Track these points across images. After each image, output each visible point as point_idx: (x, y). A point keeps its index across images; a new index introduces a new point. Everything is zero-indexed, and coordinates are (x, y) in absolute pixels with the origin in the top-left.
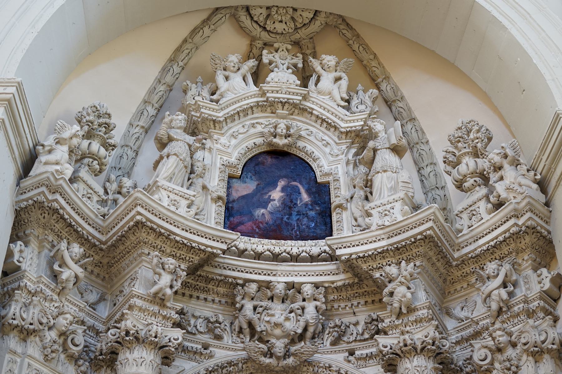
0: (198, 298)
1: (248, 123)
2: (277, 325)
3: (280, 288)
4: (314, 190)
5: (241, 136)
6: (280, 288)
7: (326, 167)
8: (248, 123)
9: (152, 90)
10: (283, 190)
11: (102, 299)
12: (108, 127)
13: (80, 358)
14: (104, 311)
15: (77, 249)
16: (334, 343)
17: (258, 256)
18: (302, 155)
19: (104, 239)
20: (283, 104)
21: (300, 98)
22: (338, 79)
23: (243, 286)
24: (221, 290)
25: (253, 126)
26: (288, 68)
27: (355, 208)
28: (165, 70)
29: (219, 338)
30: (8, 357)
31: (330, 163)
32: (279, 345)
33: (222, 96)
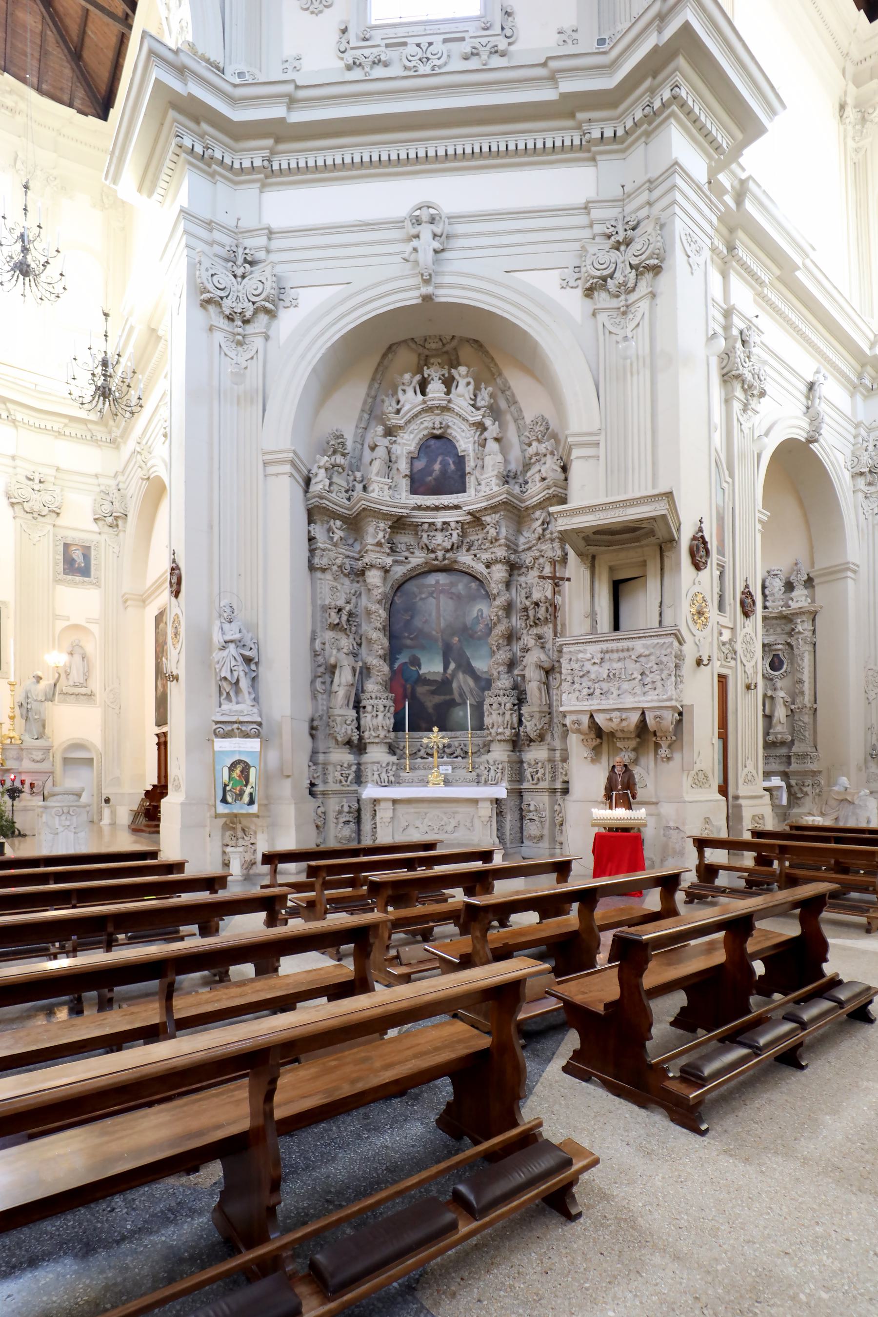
12: (343, 444)
15: (338, 523)
17: (428, 508)
18: (450, 438)
19: (350, 513)
20: (437, 407)
25: (422, 423)
27: (477, 473)
28: (370, 387)
30: (319, 582)
31: (465, 443)
32: (440, 554)
33: (403, 406)
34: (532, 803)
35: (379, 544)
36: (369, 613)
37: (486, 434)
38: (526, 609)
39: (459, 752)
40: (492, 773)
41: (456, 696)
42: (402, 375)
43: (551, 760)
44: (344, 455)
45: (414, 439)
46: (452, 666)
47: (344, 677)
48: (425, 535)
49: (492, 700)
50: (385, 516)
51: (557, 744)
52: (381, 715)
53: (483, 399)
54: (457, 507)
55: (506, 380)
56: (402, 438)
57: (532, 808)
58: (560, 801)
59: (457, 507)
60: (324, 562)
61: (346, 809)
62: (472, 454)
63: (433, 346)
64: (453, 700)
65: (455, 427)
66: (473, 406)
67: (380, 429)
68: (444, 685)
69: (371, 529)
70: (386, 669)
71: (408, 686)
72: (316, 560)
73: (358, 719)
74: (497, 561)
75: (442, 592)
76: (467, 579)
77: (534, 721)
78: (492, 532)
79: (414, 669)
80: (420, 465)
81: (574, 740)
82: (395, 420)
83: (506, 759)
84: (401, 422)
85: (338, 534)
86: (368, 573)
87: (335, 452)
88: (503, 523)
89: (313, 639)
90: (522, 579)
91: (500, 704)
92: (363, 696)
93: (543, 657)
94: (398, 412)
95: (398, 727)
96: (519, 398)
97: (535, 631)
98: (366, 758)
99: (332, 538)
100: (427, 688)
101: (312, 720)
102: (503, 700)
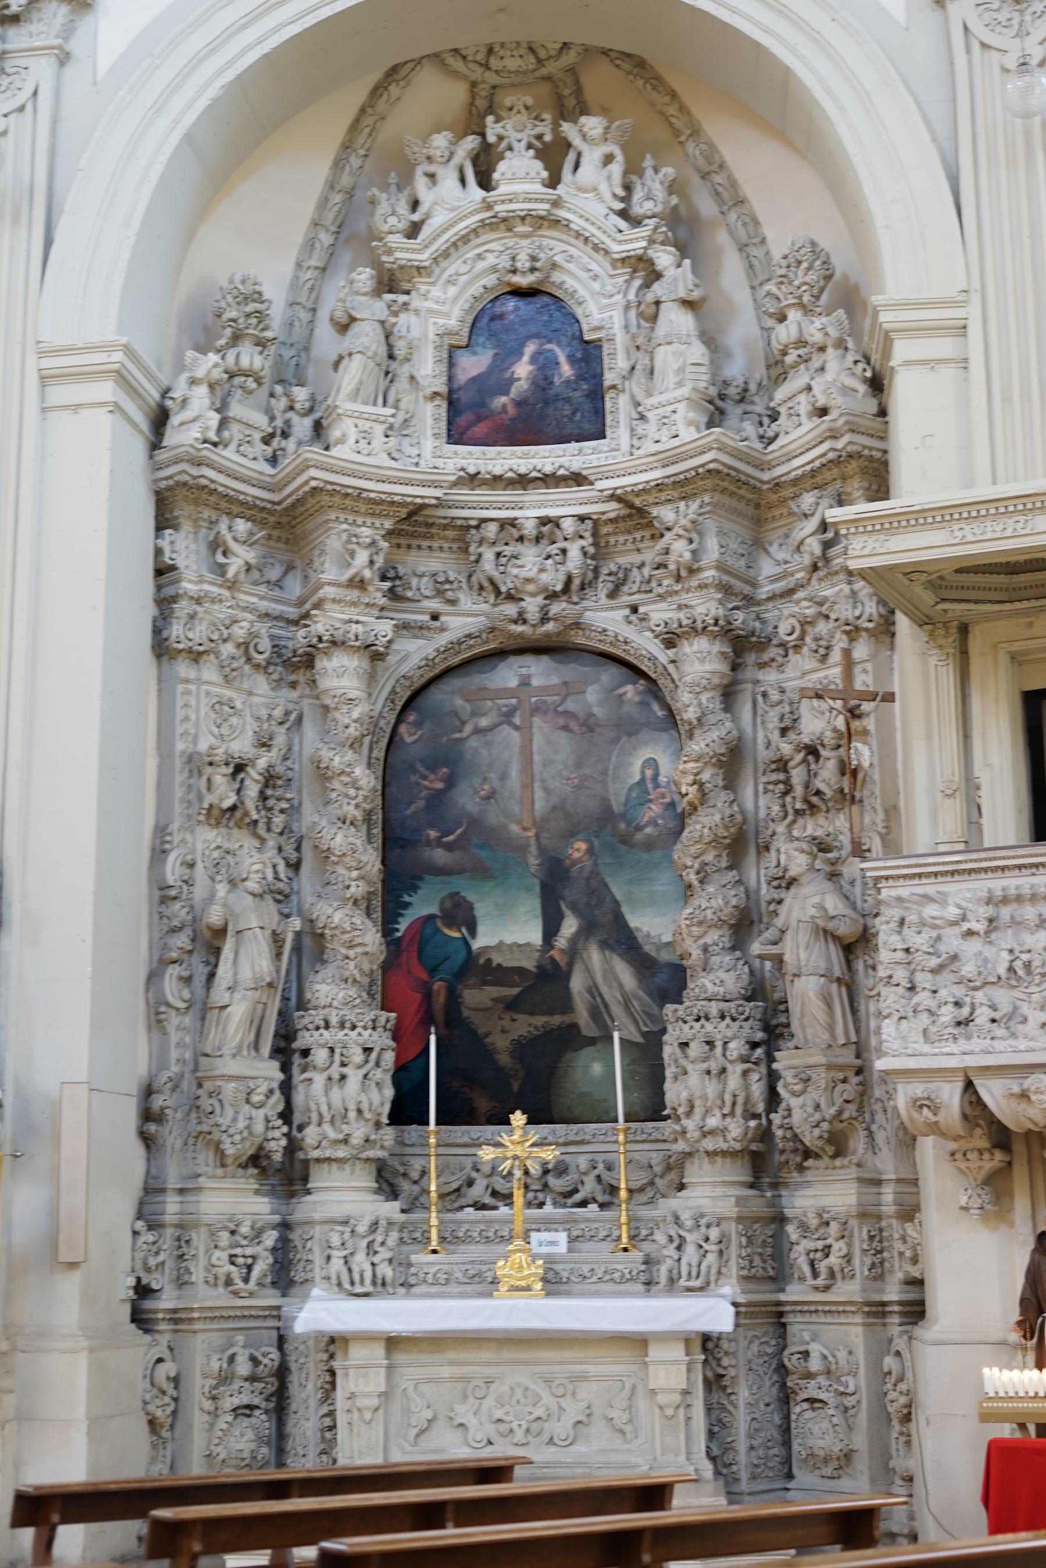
0: (419, 547)
1: (471, 255)
2: (528, 580)
3: (529, 528)
4: (579, 355)
5: (463, 279)
6: (529, 528)
7: (597, 316)
8: (471, 255)
9: (323, 203)
10: (533, 360)
11: (290, 568)
12: (261, 316)
13: (269, 663)
14: (294, 588)
15: (242, 526)
16: (612, 595)
17: (497, 481)
18: (558, 293)
19: (276, 497)
20: (523, 219)
21: (547, 206)
22: (608, 159)
23: (477, 527)
24: (450, 534)
25: (480, 257)
26: (530, 146)
27: (636, 386)
28: (338, 165)
29: (453, 602)
30: (180, 688)
31: (602, 309)
33: (428, 216)
34: (815, 1349)
35: (358, 583)
36: (323, 774)
37: (658, 289)
38: (782, 765)
39: (590, 1186)
40: (690, 1253)
41: (582, 1015)
43: (867, 1214)
44: (261, 343)
45: (455, 299)
46: (570, 926)
48: (489, 555)
49: (686, 1031)
50: (377, 506)
51: (886, 1163)
53: (649, 197)
54: (577, 479)
55: (712, 147)
56: (425, 296)
57: (815, 1364)
58: (900, 1344)
59: (577, 479)
60: (200, 633)
61: (243, 1368)
62: (621, 339)
63: (512, 64)
64: (574, 1027)
65: (571, 266)
66: (623, 214)
67: (365, 276)
69: (334, 543)
70: (372, 938)
71: (437, 985)
72: (176, 630)
73: (286, 1088)
74: (695, 630)
75: (536, 710)
76: (610, 674)
77: (814, 1094)
78: (680, 550)
79: (455, 934)
81: (928, 1148)
83: (728, 1207)
84: (424, 257)
85: (242, 556)
86: (322, 663)
87: (237, 338)
88: (711, 525)
89: (159, 853)
90: (770, 676)
91: (710, 1043)
92: (302, 1020)
93: (833, 904)
94: (414, 230)
96: (748, 190)
97: (812, 827)
98: (307, 1207)
99: (221, 569)
100: (494, 991)
101: (148, 1091)
102: (718, 1030)
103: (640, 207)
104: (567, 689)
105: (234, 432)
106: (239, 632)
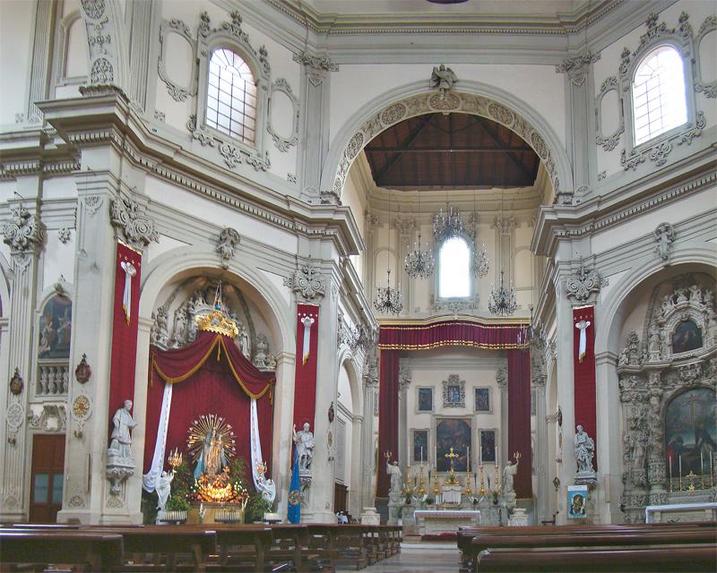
12: (636, 338)
17: (682, 359)
32: (690, 382)
42: (663, 297)
47: (639, 452)
52: (658, 471)
68: (695, 451)
72: (624, 397)
80: (677, 338)
82: (661, 320)
95: (668, 476)
98: (652, 492)
103: (706, 300)
104: (700, 395)
105: (632, 360)
106: (635, 396)
